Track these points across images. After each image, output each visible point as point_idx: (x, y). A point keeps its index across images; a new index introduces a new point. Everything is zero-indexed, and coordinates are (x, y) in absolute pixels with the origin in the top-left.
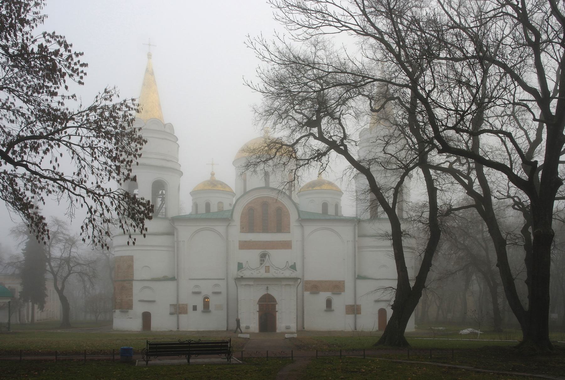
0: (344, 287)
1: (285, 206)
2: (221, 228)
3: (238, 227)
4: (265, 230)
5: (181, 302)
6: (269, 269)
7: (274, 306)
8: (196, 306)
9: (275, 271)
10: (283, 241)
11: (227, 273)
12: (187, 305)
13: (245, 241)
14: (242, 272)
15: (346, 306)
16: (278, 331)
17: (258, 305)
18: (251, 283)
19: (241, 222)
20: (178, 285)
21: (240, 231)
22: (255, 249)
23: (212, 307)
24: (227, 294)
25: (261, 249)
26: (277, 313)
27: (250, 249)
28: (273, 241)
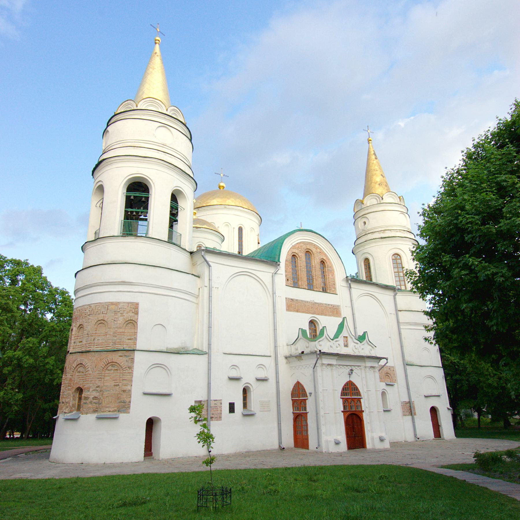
1: (329, 259)
3: (284, 279)
4: (310, 287)
9: (355, 344)
10: (332, 305)
11: (276, 347)
13: (291, 299)
17: (341, 400)
18: (333, 361)
19: (286, 271)
20: (209, 363)
21: (285, 284)
22: (303, 312)
24: (277, 382)
25: (310, 313)
26: (363, 413)
27: (297, 311)
28: (321, 304)
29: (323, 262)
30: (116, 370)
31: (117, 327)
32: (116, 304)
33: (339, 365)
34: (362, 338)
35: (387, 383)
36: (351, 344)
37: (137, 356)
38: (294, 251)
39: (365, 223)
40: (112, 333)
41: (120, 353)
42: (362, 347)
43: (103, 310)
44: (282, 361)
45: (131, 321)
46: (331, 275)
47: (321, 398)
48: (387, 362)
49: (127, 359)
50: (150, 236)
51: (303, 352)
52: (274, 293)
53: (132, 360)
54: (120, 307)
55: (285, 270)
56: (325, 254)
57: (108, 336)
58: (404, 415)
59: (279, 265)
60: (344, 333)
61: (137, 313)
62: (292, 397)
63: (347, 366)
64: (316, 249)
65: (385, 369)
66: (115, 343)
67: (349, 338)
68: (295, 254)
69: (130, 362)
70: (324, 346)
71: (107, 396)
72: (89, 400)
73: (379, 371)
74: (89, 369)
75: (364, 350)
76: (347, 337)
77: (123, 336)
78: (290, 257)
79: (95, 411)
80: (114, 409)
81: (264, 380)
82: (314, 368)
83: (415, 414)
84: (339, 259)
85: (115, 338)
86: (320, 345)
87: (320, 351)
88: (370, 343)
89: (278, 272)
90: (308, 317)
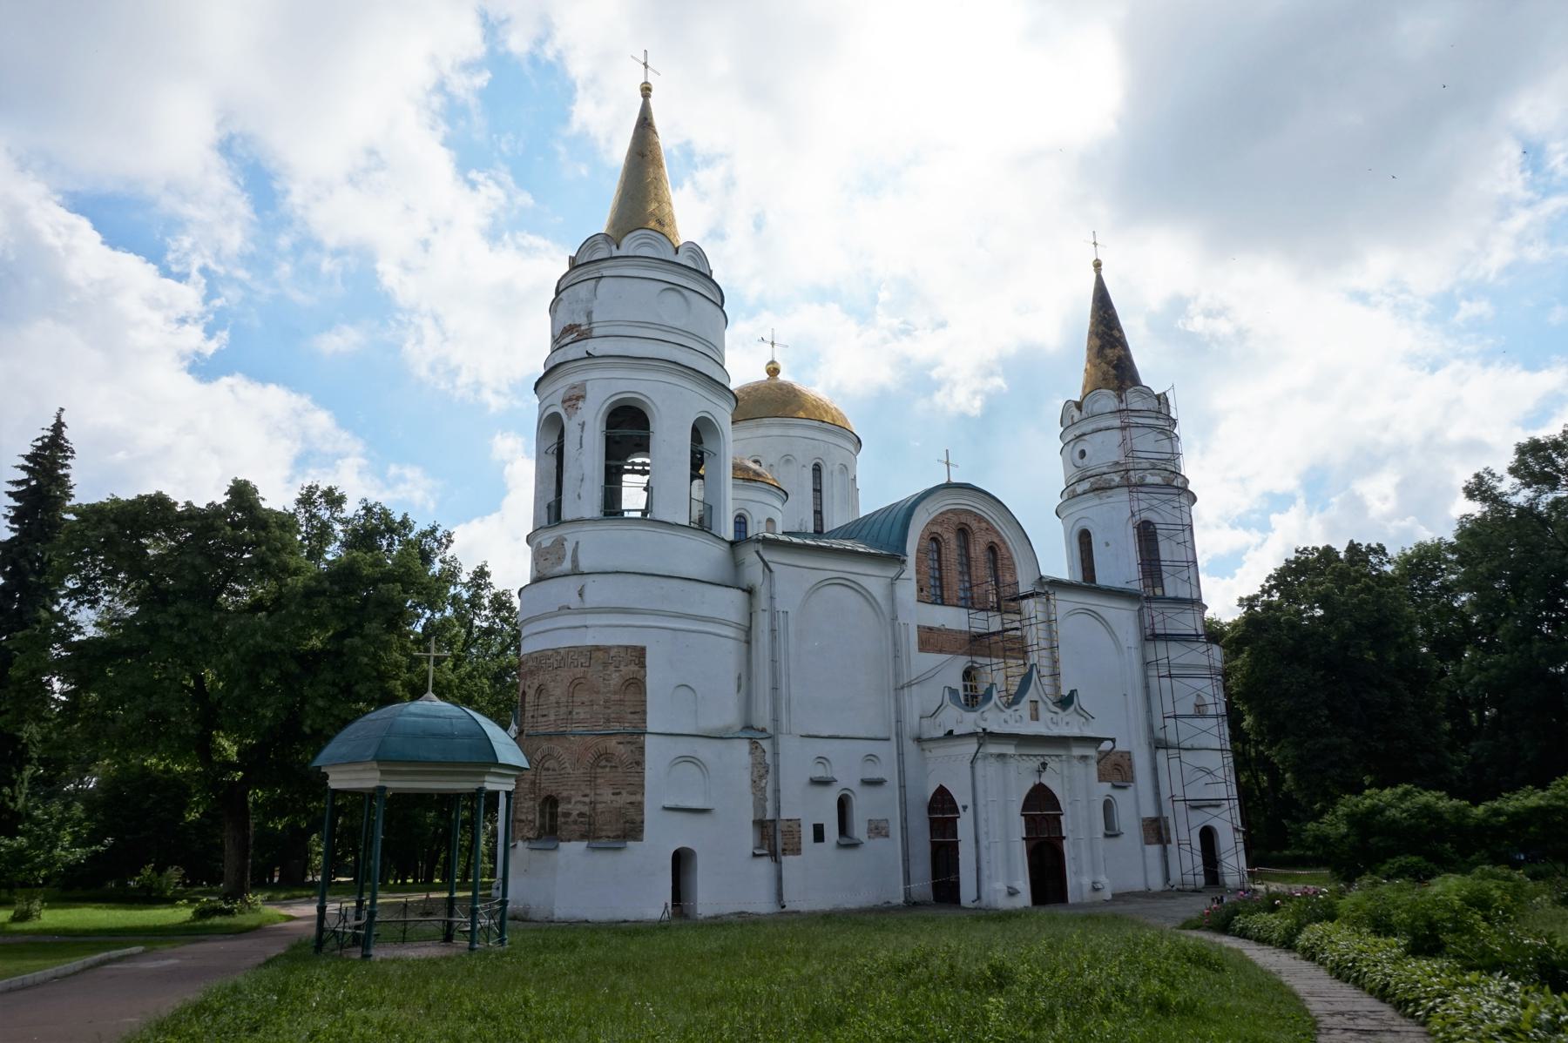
0: (1131, 766)
1: (1005, 543)
2: (874, 579)
5: (784, 816)
6: (1036, 710)
7: (1057, 818)
8: (822, 825)
12: (798, 822)
13: (930, 629)
14: (986, 715)
15: (1144, 820)
16: (1072, 897)
17: (1023, 818)
18: (1009, 749)
19: (918, 572)
23: (859, 829)
24: (902, 787)
26: (1064, 842)
29: (992, 549)
30: (616, 767)
31: (609, 692)
32: (606, 649)
33: (1020, 755)
34: (1065, 702)
35: (1116, 784)
36: (1044, 714)
37: (649, 741)
38: (934, 529)
39: (1083, 454)
40: (602, 703)
41: (620, 739)
42: (1067, 719)
43: (583, 661)
44: (910, 747)
45: (634, 681)
46: (1008, 575)
47: (982, 816)
48: (1114, 747)
49: (633, 747)
50: (658, 518)
51: (951, 732)
52: (895, 618)
53: (642, 749)
54: (612, 654)
55: (917, 570)
56: (997, 532)
57: (595, 707)
58: (1148, 843)
59: (904, 562)
60: (1032, 694)
61: (643, 665)
62: (929, 813)
63: (1035, 756)
64: (979, 522)
65: (1113, 757)
66: (608, 721)
67: (1041, 705)
68: (936, 535)
69: (637, 753)
70: (994, 718)
71: (602, 812)
72: (571, 819)
73: (1098, 763)
74: (567, 765)
75: (1068, 725)
76: (1036, 702)
77: (622, 708)
78: (925, 543)
79: (582, 837)
80: (615, 834)
81: (878, 783)
82: (972, 762)
83: (1169, 841)
84: (1026, 541)
85: (609, 711)
86: (985, 720)
87: (984, 730)
88: (1082, 712)
89: (901, 577)
90: (962, 662)
